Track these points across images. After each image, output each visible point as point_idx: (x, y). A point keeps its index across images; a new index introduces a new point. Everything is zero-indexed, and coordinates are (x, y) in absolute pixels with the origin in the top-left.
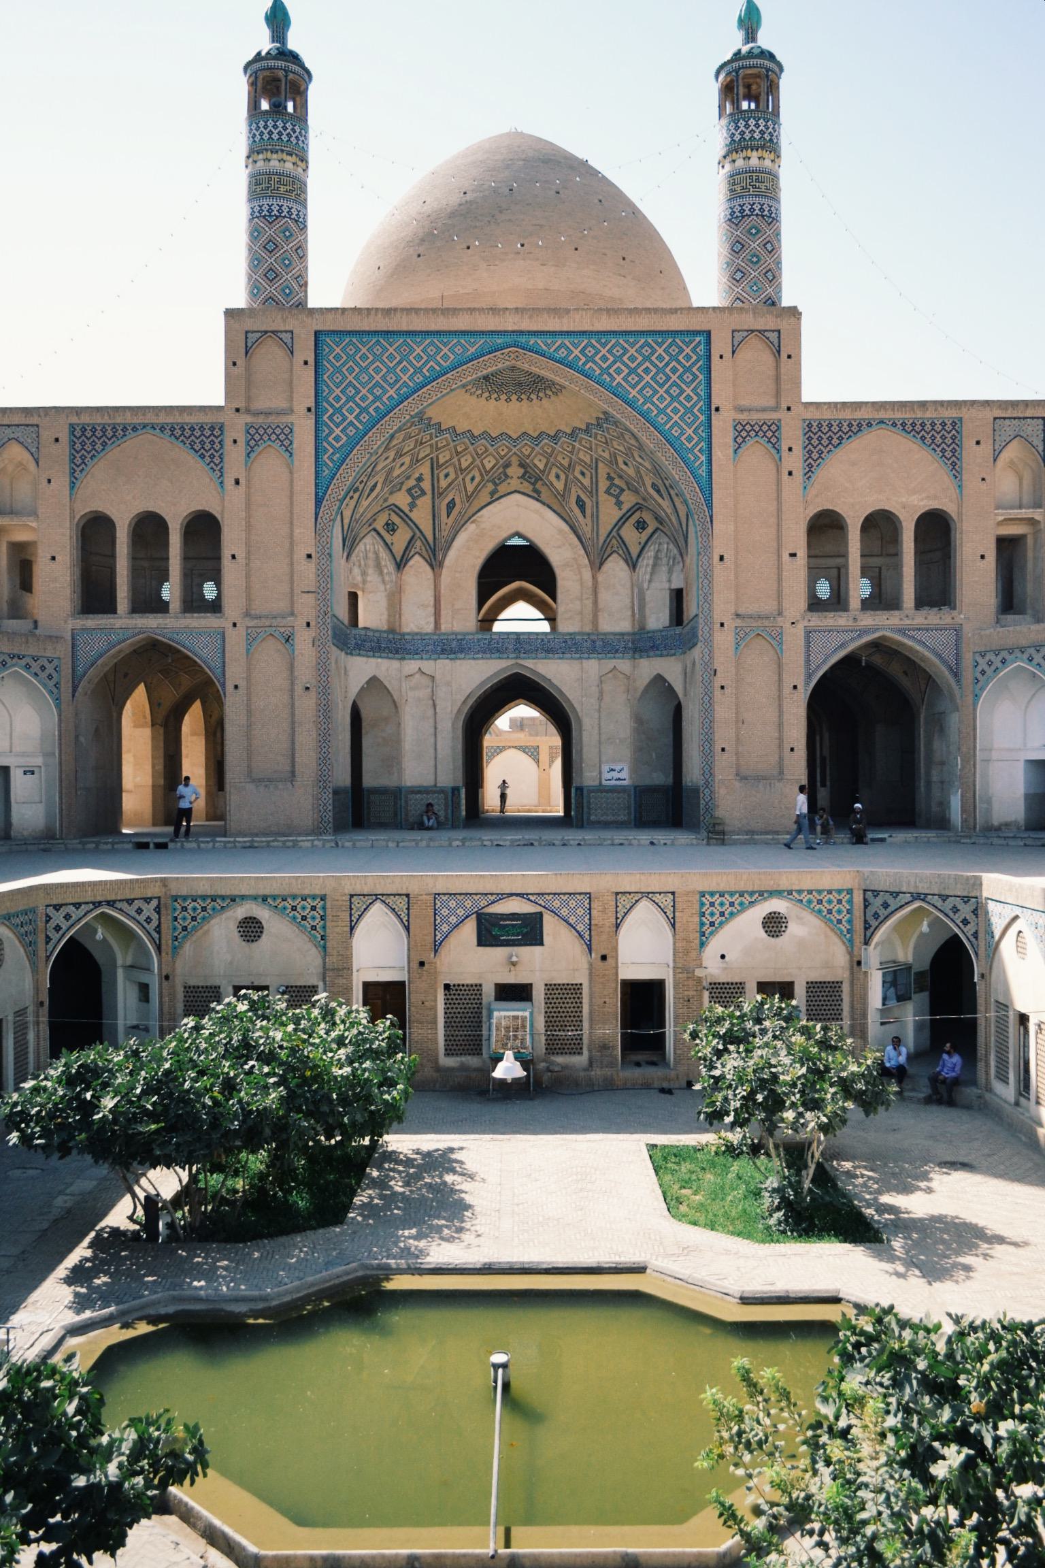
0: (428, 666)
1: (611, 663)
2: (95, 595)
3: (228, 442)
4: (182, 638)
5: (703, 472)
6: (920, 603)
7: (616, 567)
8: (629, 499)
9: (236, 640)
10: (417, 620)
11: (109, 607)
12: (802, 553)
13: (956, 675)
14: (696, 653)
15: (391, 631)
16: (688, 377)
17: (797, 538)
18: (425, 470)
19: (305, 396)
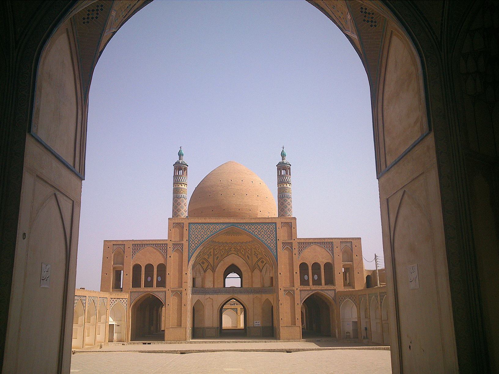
0: (211, 296)
1: (255, 295)
2: (136, 283)
3: (168, 248)
4: (156, 293)
5: (275, 254)
6: (326, 284)
7: (257, 272)
8: (259, 256)
9: (169, 294)
10: (209, 284)
11: (140, 286)
12: (298, 273)
13: (335, 301)
14: (275, 294)
15: (203, 287)
16: (272, 233)
17: (297, 269)
18: (212, 250)
19: (186, 238)
